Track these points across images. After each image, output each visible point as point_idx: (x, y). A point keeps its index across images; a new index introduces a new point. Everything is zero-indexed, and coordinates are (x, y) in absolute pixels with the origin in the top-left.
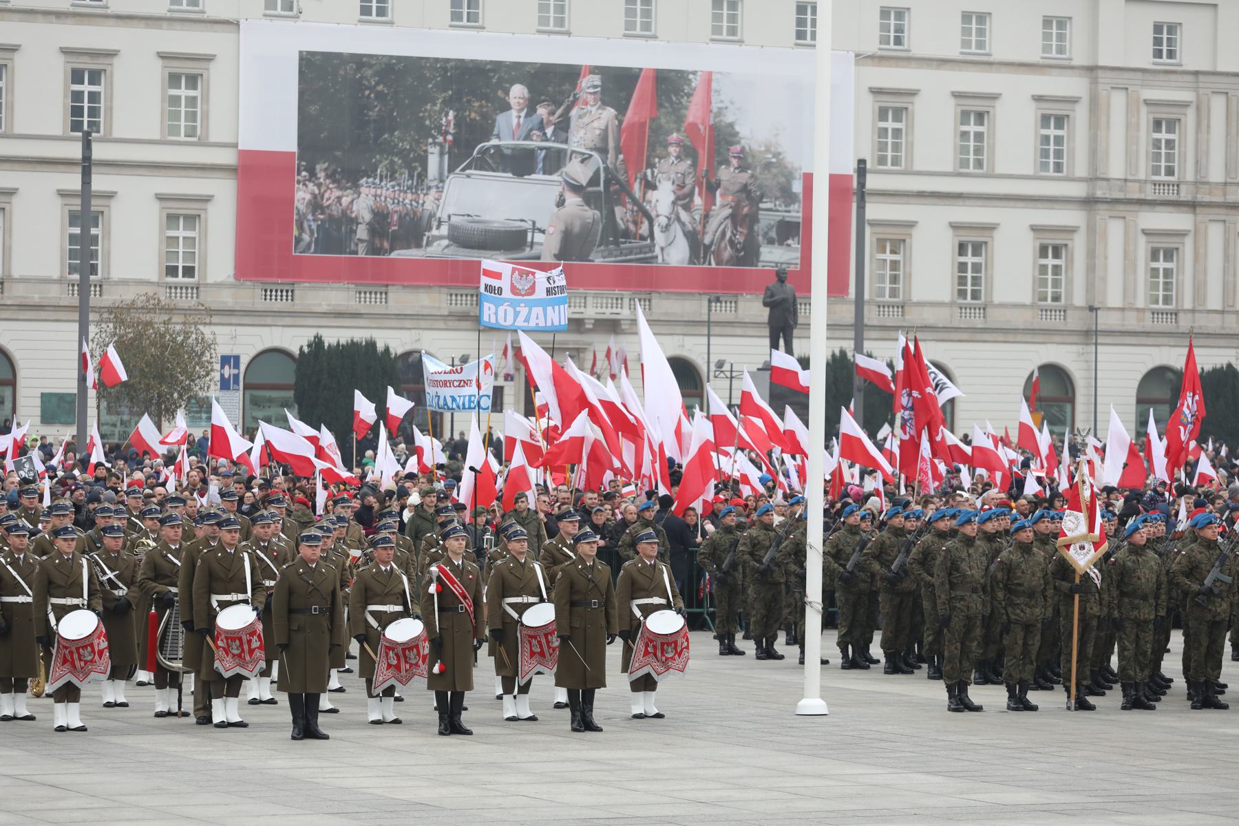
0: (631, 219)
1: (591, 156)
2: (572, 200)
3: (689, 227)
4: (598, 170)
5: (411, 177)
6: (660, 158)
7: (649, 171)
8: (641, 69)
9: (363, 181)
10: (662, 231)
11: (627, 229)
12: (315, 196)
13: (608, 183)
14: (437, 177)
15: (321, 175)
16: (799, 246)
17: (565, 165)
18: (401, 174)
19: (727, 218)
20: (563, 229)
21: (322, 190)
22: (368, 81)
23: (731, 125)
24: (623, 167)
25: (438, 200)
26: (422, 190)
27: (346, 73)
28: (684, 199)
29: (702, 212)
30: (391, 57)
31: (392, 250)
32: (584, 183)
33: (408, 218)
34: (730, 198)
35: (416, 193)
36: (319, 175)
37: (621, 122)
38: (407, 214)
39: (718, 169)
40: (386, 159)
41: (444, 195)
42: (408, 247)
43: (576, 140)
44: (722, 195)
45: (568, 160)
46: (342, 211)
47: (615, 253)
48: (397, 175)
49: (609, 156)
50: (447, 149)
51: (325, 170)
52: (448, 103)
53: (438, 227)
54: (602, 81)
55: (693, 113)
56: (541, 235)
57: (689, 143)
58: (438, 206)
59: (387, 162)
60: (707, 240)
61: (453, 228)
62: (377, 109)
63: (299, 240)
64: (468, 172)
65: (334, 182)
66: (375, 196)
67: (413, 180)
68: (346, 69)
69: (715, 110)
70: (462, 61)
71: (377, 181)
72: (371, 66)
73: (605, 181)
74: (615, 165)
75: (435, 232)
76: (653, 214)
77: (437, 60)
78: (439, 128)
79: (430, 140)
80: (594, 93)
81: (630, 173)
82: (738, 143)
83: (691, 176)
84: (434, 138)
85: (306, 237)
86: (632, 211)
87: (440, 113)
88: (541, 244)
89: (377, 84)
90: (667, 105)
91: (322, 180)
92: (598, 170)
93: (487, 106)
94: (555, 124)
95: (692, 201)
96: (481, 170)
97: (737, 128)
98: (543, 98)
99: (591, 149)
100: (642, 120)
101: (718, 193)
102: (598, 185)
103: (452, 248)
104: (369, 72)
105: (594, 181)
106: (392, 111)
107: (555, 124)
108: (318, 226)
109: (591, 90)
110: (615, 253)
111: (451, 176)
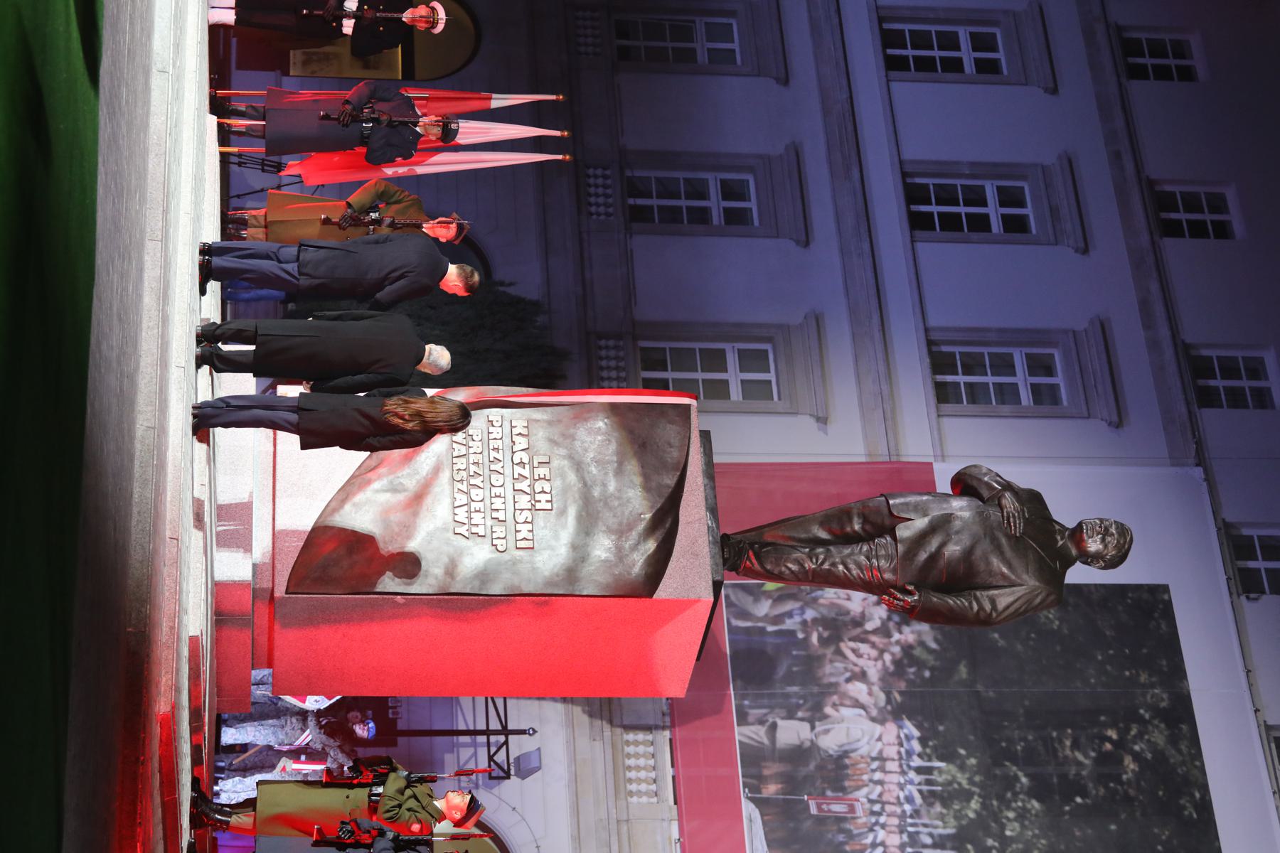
9: (910, 728)
15: (908, 634)
18: (942, 817)
22: (1140, 736)
27: (1143, 686)
30: (1205, 788)
31: (759, 803)
33: (841, 838)
36: (906, 629)
38: (848, 833)
40: (971, 781)
46: (836, 685)
48: (938, 808)
51: (922, 644)
59: (965, 783)
62: (1080, 757)
63: (756, 594)
65: (897, 663)
66: (881, 758)
68: (1153, 686)
71: (917, 762)
72: (1174, 740)
89: (1137, 757)
91: (896, 636)
104: (1159, 737)
106: (1084, 795)
108: (792, 633)
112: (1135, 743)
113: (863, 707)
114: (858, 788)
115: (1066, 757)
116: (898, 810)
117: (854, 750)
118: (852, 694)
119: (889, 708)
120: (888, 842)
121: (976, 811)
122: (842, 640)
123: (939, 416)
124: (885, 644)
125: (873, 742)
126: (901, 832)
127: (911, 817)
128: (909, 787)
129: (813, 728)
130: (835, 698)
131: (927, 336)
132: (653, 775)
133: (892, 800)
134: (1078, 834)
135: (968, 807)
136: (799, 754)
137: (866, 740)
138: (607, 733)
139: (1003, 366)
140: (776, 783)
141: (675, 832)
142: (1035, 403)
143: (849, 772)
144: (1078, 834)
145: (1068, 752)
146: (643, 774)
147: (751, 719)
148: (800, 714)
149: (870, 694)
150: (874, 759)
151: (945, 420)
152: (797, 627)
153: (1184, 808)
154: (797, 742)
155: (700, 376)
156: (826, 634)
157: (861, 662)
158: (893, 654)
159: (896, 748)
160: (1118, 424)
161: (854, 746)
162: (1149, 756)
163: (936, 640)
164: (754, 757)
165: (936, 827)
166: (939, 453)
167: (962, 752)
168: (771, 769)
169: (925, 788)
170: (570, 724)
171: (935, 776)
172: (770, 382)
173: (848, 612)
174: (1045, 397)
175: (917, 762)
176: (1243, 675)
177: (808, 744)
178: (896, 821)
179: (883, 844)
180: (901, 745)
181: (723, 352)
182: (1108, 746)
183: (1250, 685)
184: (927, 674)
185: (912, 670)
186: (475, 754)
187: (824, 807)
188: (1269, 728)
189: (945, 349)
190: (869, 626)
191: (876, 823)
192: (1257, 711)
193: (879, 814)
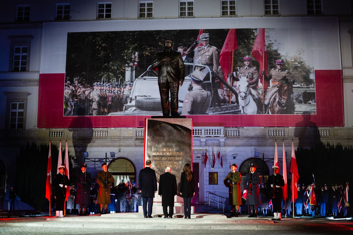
0: (226, 94)
1: (205, 67)
2: (196, 87)
3: (257, 97)
4: (209, 73)
5: (117, 81)
6: (240, 67)
7: (234, 73)
8: (229, 29)
10: (242, 99)
11: (225, 99)
12: (73, 91)
13: (213, 79)
14: (130, 80)
15: (76, 82)
16: (316, 104)
17: (192, 72)
18: (113, 80)
19: (276, 92)
20: (192, 101)
21: (76, 89)
23: (276, 51)
24: (221, 71)
25: (130, 90)
26: (123, 86)
28: (253, 84)
29: (263, 90)
31: (108, 113)
32: (202, 80)
33: (116, 98)
34: (277, 83)
35: (120, 87)
36: (75, 82)
37: (219, 52)
38: (115, 97)
39: (270, 70)
40: (106, 74)
41: (133, 88)
42: (116, 111)
43: (197, 61)
44: (272, 82)
45: (193, 70)
46: (86, 97)
47: (219, 110)
48: (111, 80)
49: (214, 67)
50: (134, 69)
51: (78, 80)
52: (135, 49)
53: (130, 102)
54: (209, 35)
55: (256, 46)
56: (181, 103)
57: (255, 60)
58: (130, 93)
59: (106, 75)
60: (266, 102)
61: (137, 102)
63: (66, 110)
64: (144, 77)
65: (81, 85)
67: (118, 82)
69: (267, 44)
70: (142, 31)
71: (102, 83)
73: (212, 78)
74: (217, 71)
75: (129, 104)
76: (238, 92)
77: (130, 32)
78: (131, 60)
79: (127, 65)
80: (206, 41)
81: (225, 74)
82: (280, 58)
83: (256, 74)
84: (128, 64)
85: (69, 109)
86: (227, 91)
87: (131, 53)
88: (181, 107)
89: (102, 43)
90: (242, 44)
91: (76, 84)
92: (209, 73)
93: (154, 49)
94: (186, 55)
95: (257, 85)
96: (150, 76)
97: (279, 52)
98: (180, 44)
99: (205, 65)
100: (230, 51)
101: (271, 81)
102: (209, 80)
103: (138, 110)
105: (207, 78)
107: (186, 55)
108: (75, 104)
109: (204, 40)
110: (219, 110)
111: (137, 79)
112: (100, 43)
113: (90, 92)
114: (106, 94)
115: (102, 56)
116: (111, 88)
117: (99, 94)
118: (88, 94)
119: (91, 87)
120: (117, 90)
121: (112, 74)
122: (77, 95)
123: (29, 71)
124: (78, 87)
125: (97, 91)
126: (115, 88)
127: (112, 85)
128: (107, 85)
129: (94, 102)
130: (88, 97)
131: (11, 72)
132: (102, 132)
133: (109, 88)
134: (117, 56)
135: (111, 75)
136: (99, 104)
137: (97, 92)
138: (94, 140)
139: (18, 58)
140: (105, 109)
141: (114, 128)
142: (27, 52)
143: (103, 96)
144: (117, 56)
145: (101, 56)
146: (101, 134)
147: (92, 113)
148: (91, 104)
149: (88, 90)
150: (101, 91)
151: (30, 70)
152: (73, 103)
153: (112, 36)
154: (97, 105)
155: (17, 117)
156: (75, 98)
157: (81, 91)
158: (80, 85)
159: (99, 87)
160: (32, 37)
161: (98, 94)
162: (102, 41)
163: (77, 77)
164: (99, 113)
165: (115, 81)
166: (38, 72)
167: (100, 75)
168: (102, 110)
169: (107, 82)
170: (91, 146)
171: (105, 80)
172: (19, 104)
173: (71, 93)
174: (26, 50)
175: (102, 83)
176: (86, 22)
177: (97, 103)
178: (113, 88)
179: (117, 91)
180: (98, 86)
181: (12, 112)
182: (100, 48)
183: (88, 21)
184: (84, 79)
185: (83, 82)
186: (97, 164)
187: (110, 101)
188: (97, 19)
189: (13, 68)
190: (74, 89)
191: (113, 92)
192: (94, 20)
193: (112, 91)
